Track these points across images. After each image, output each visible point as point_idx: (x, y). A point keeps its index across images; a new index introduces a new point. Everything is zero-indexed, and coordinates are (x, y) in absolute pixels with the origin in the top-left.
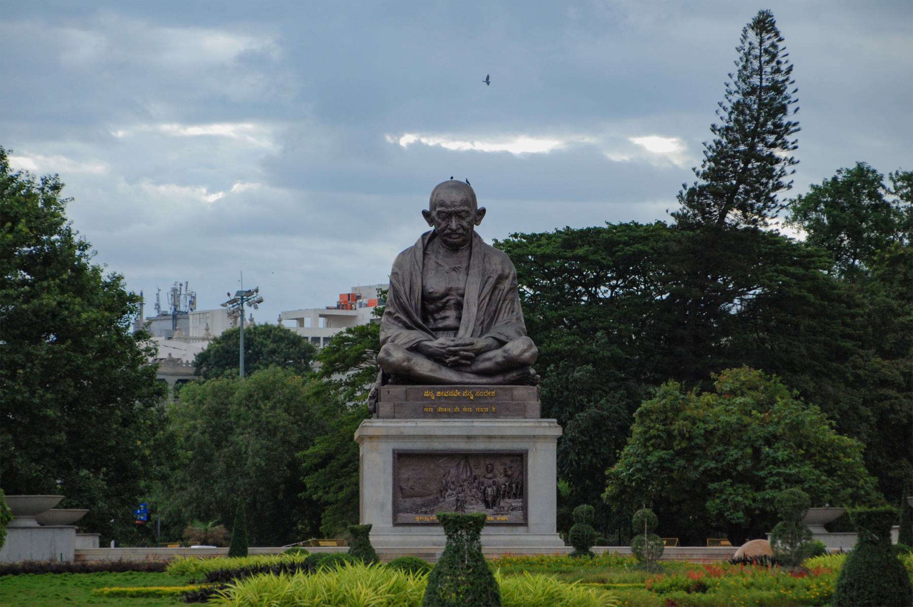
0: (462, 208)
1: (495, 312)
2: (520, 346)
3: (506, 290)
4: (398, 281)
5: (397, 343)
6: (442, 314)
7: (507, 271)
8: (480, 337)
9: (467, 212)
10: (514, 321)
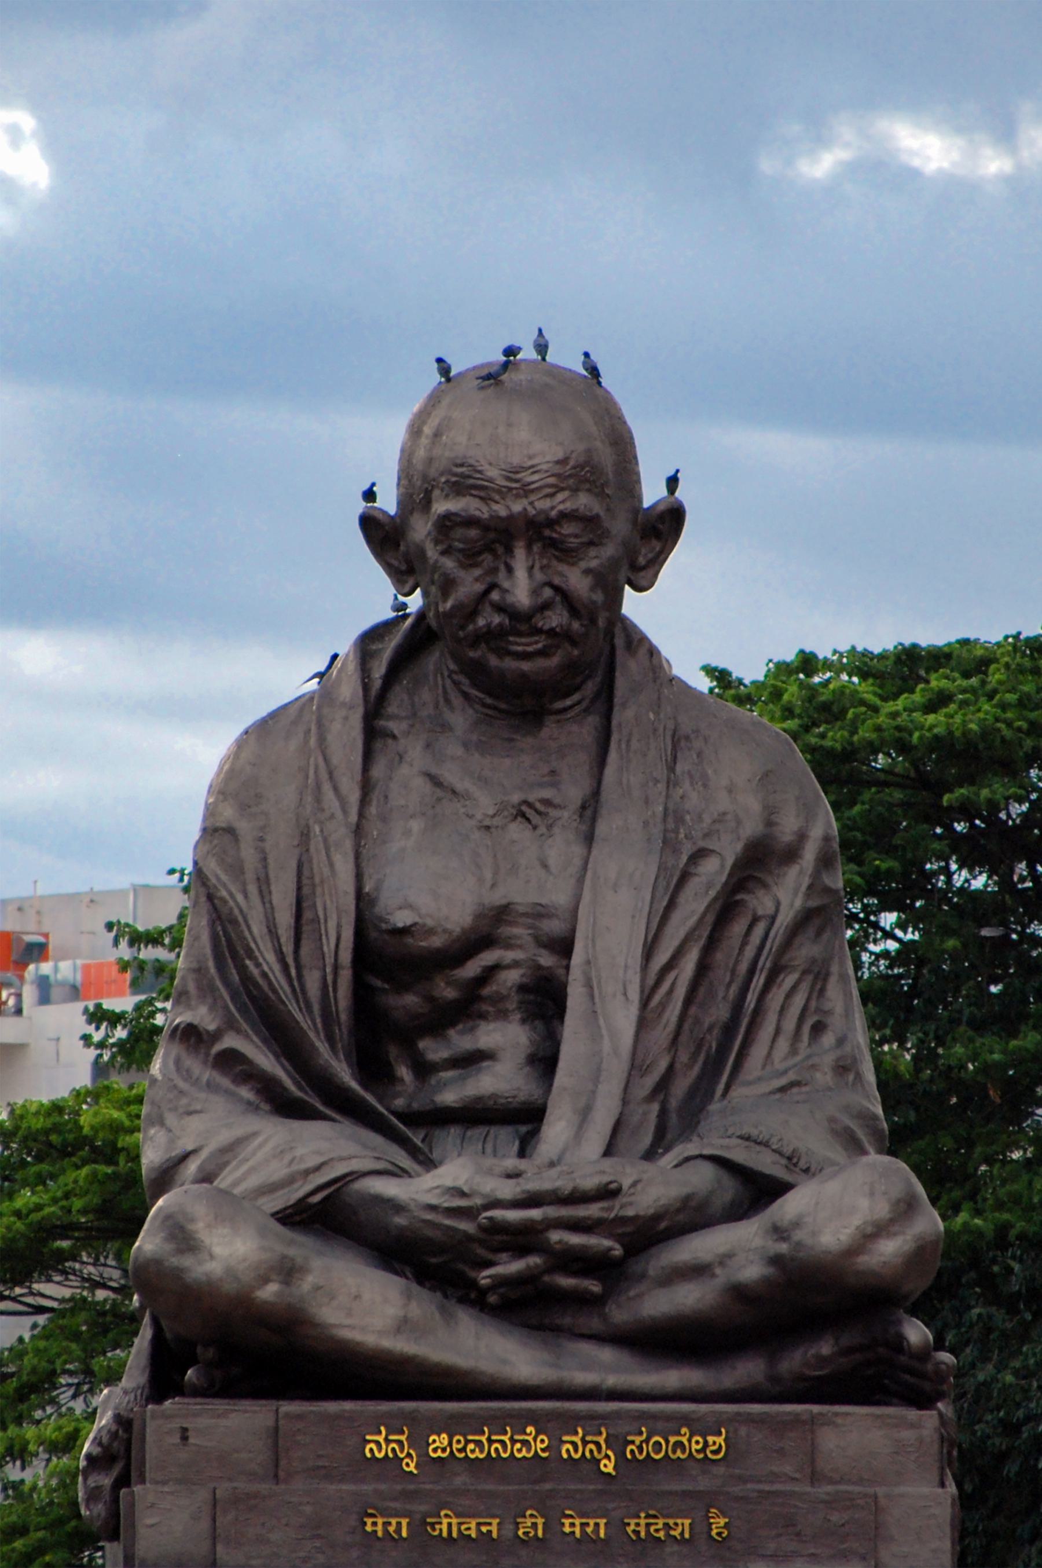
0: (562, 502)
1: (729, 1029)
2: (853, 1206)
3: (785, 918)
4: (237, 870)
5: (229, 1192)
6: (461, 1041)
7: (788, 826)
8: (650, 1155)
9: (590, 521)
10: (824, 1077)
